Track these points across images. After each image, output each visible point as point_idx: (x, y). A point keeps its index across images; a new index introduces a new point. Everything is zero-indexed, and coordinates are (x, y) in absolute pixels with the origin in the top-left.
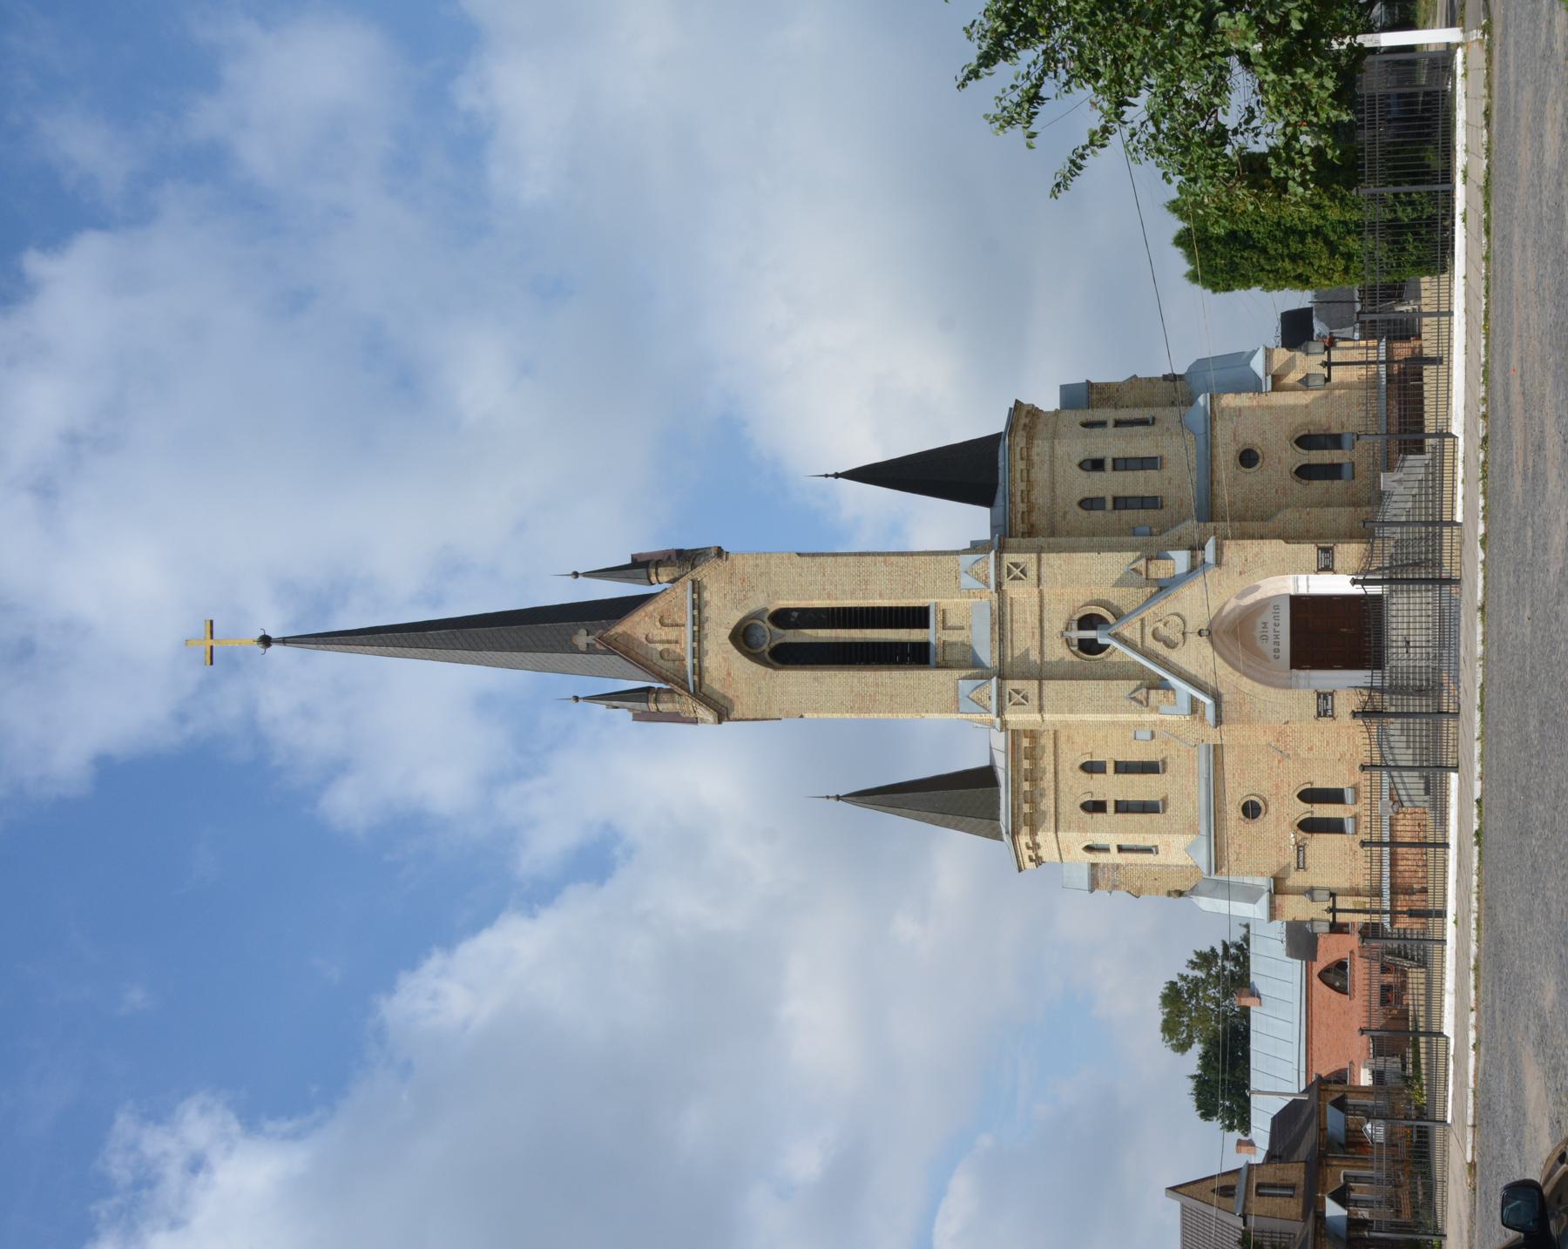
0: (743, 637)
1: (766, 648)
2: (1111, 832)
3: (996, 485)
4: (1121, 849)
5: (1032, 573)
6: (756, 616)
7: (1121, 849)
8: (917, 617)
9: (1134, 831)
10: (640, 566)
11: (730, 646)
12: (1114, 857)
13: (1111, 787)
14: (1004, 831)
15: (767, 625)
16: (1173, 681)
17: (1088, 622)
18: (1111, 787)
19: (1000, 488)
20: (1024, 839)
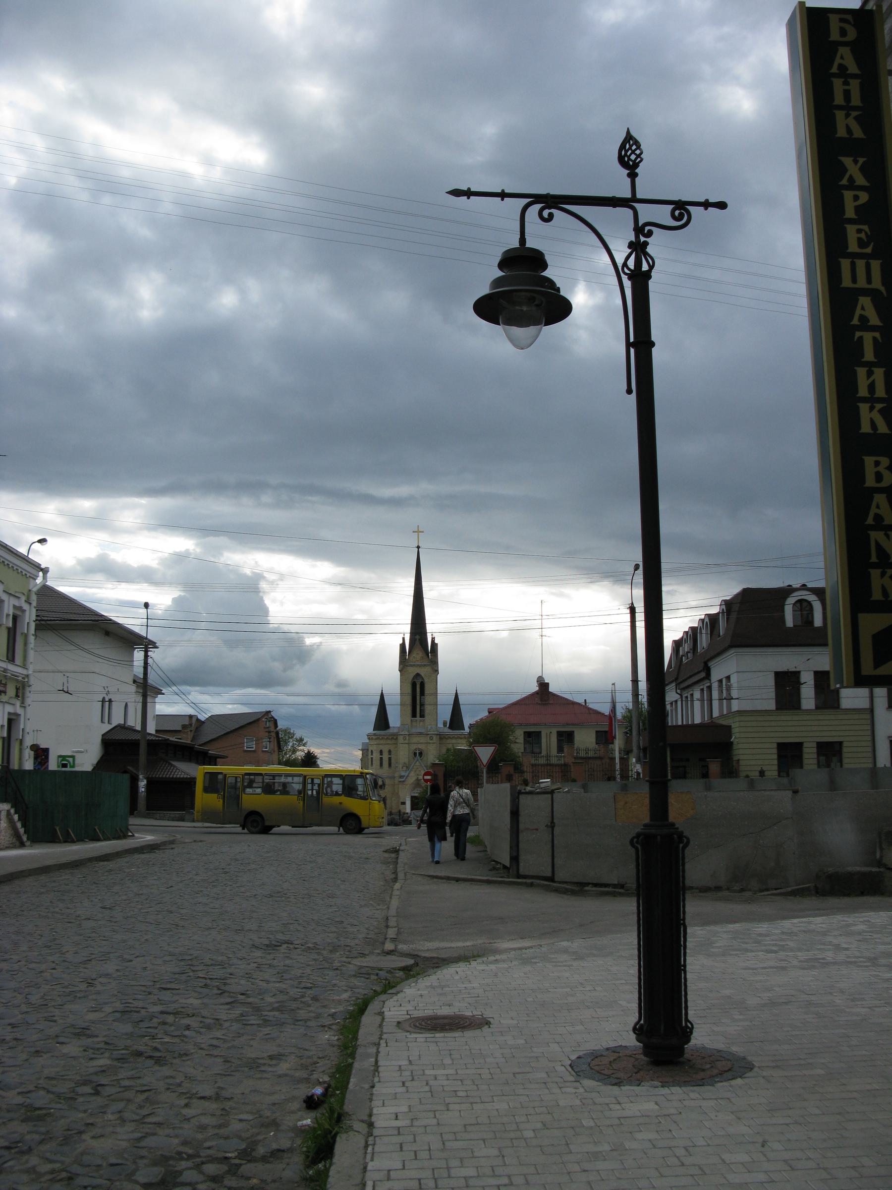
0: (418, 675)
1: (415, 680)
2: (376, 756)
3: (453, 730)
4: (372, 758)
5: (431, 742)
6: (423, 679)
7: (372, 758)
8: (422, 716)
9: (377, 762)
10: (434, 645)
11: (414, 674)
12: (370, 756)
13: (386, 757)
14: (375, 732)
15: (421, 681)
16: (408, 772)
17: (421, 754)
18: (386, 757)
19: (451, 731)
20: (374, 737)
